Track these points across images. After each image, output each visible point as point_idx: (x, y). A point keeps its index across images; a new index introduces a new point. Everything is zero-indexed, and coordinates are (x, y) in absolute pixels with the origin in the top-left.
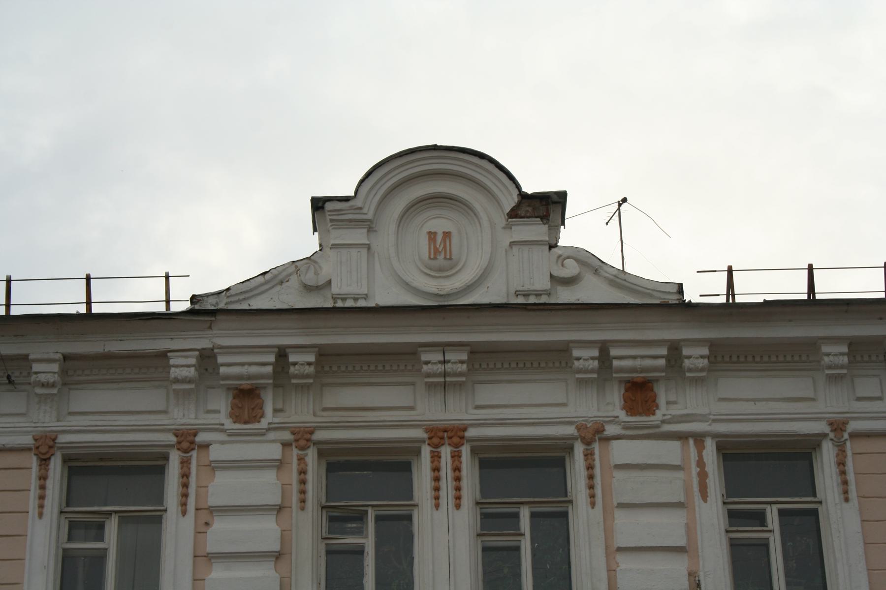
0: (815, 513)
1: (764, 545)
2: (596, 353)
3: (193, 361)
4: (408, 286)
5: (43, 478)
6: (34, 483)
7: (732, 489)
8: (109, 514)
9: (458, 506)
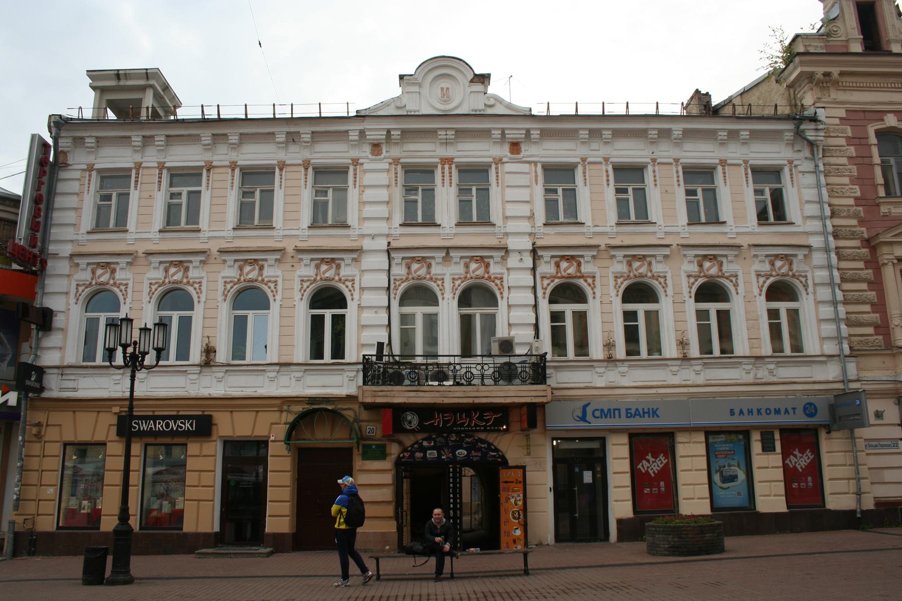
0: (574, 190)
1: (557, 201)
2: (500, 132)
3: (357, 134)
4: (433, 107)
5: (306, 175)
6: (303, 177)
7: (547, 180)
8: (329, 187)
9: (451, 186)
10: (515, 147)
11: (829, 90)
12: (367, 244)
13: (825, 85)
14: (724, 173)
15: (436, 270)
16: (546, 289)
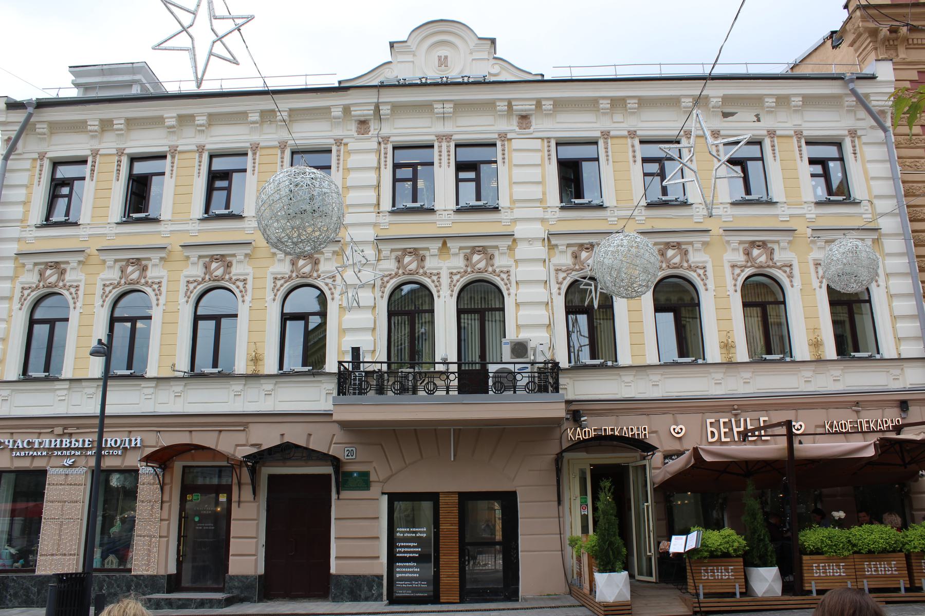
3: (341, 109)
10: (524, 118)
11: (897, 49)
13: (891, 43)
14: (773, 146)
15: (431, 263)
16: (561, 283)
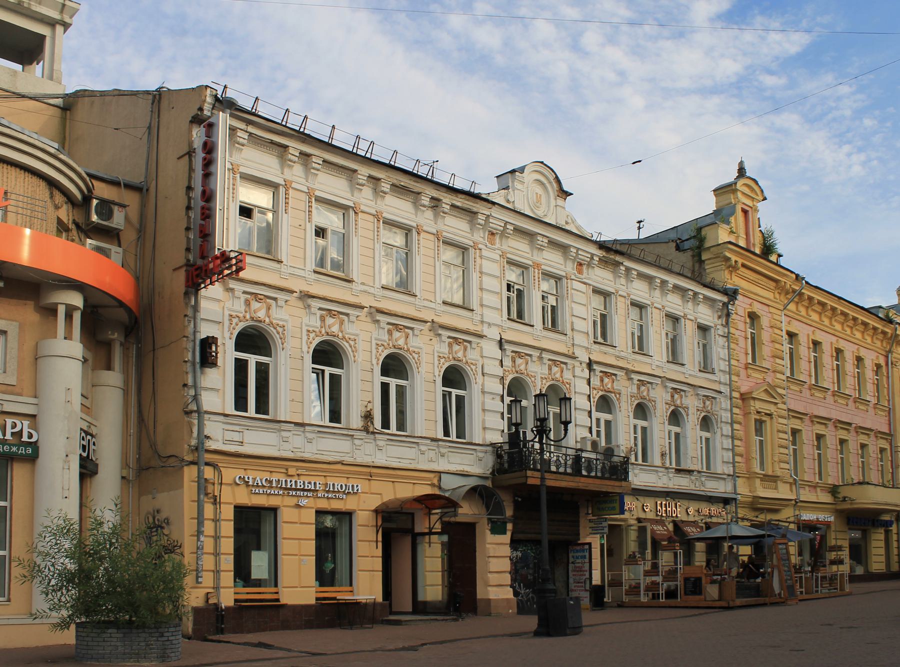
12: (486, 331)
